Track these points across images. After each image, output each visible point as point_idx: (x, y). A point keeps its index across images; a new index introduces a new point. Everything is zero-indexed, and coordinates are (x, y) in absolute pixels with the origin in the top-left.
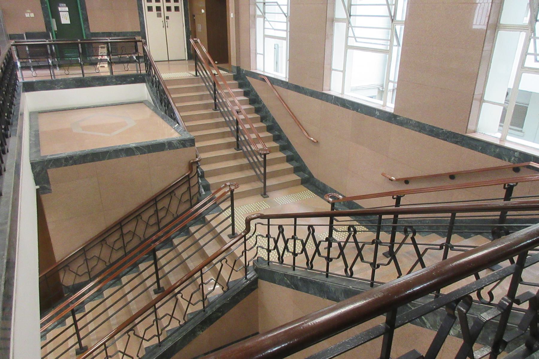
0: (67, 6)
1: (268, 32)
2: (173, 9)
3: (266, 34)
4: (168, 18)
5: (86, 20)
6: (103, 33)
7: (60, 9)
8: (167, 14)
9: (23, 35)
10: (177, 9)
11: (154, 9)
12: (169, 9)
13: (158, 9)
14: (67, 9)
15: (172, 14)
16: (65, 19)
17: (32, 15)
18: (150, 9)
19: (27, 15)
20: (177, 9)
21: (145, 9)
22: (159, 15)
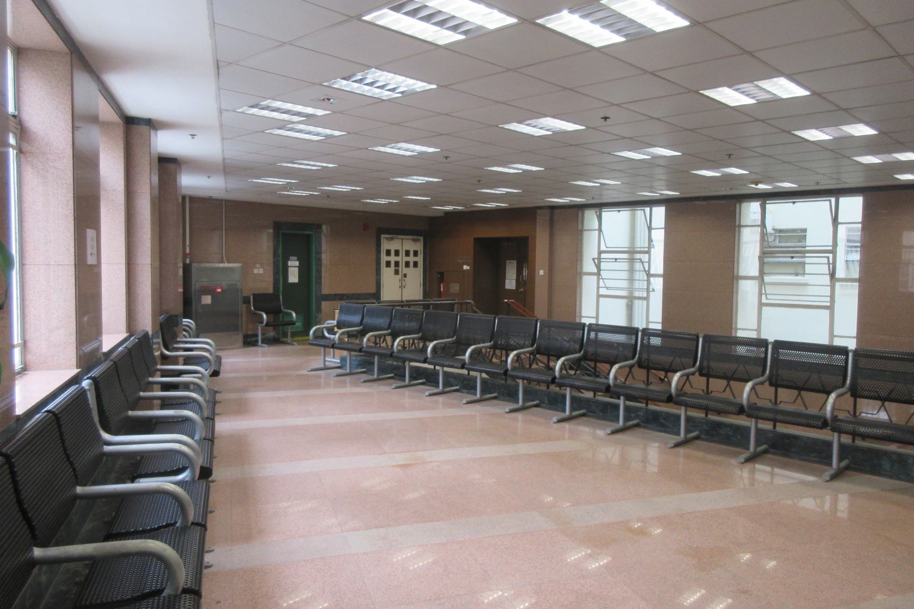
0: (298, 260)
1: (603, 291)
2: (412, 264)
3: (601, 293)
4: (405, 276)
5: (319, 278)
6: (335, 295)
7: (290, 263)
8: (405, 270)
9: (249, 297)
10: (416, 264)
11: (393, 264)
12: (407, 264)
13: (397, 264)
14: (297, 263)
15: (410, 271)
16: (293, 277)
17: (261, 271)
18: (388, 264)
19: (256, 271)
20: (416, 264)
21: (383, 264)
22: (397, 272)
